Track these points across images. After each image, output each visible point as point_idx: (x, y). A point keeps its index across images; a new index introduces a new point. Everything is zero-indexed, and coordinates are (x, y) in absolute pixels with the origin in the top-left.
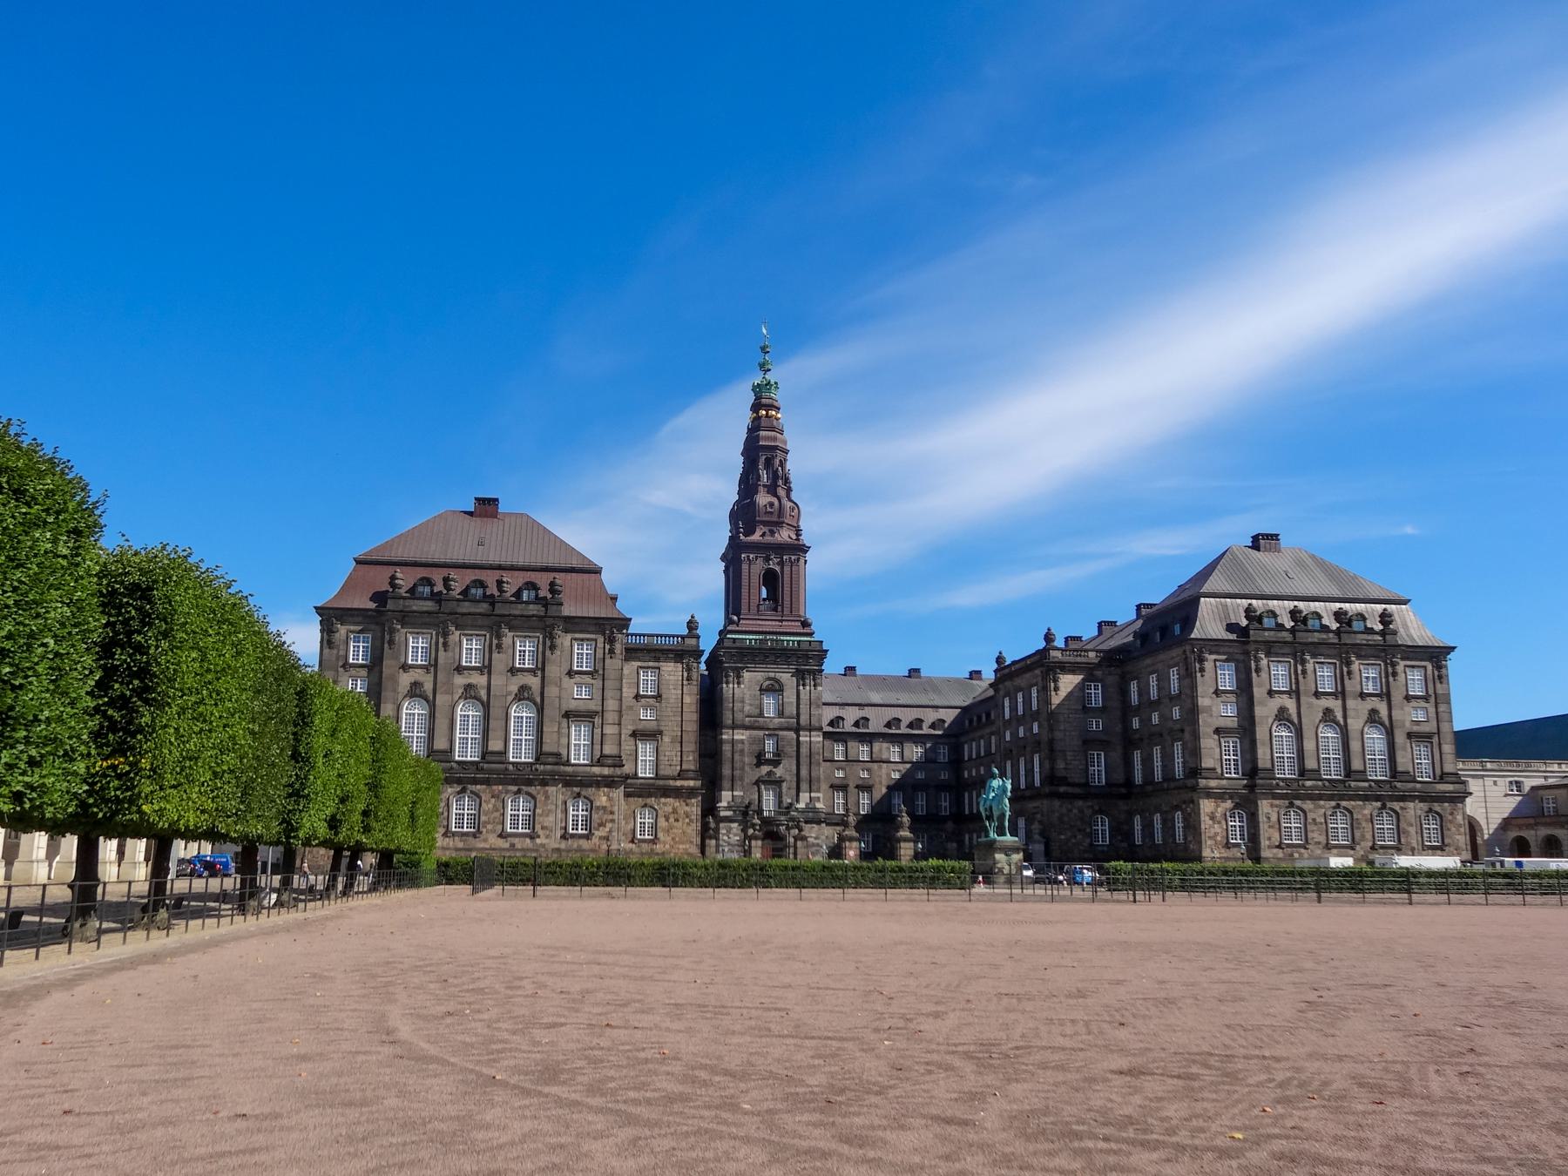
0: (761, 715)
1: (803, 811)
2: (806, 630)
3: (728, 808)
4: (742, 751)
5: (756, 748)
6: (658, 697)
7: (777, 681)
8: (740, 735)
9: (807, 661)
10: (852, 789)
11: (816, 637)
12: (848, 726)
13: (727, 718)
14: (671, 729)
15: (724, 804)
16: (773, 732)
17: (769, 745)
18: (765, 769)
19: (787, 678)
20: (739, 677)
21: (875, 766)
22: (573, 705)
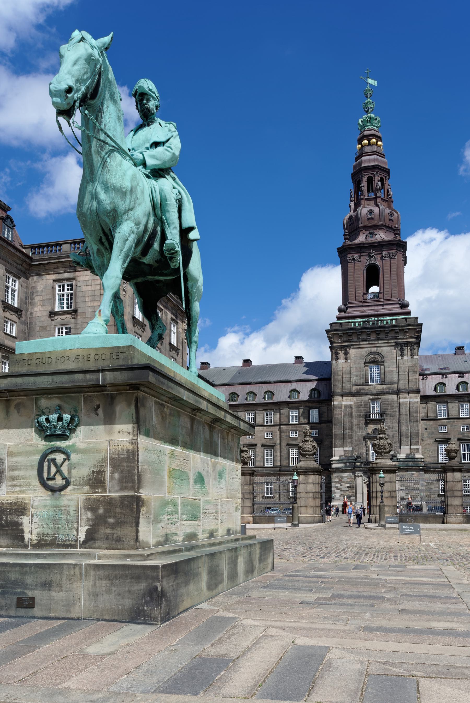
0: (366, 383)
1: (404, 461)
2: (404, 310)
3: (340, 461)
4: (351, 414)
5: (362, 410)
7: (379, 354)
8: (347, 401)
13: (338, 387)
17: (375, 408)
18: (371, 427)
19: (388, 351)
20: (346, 354)
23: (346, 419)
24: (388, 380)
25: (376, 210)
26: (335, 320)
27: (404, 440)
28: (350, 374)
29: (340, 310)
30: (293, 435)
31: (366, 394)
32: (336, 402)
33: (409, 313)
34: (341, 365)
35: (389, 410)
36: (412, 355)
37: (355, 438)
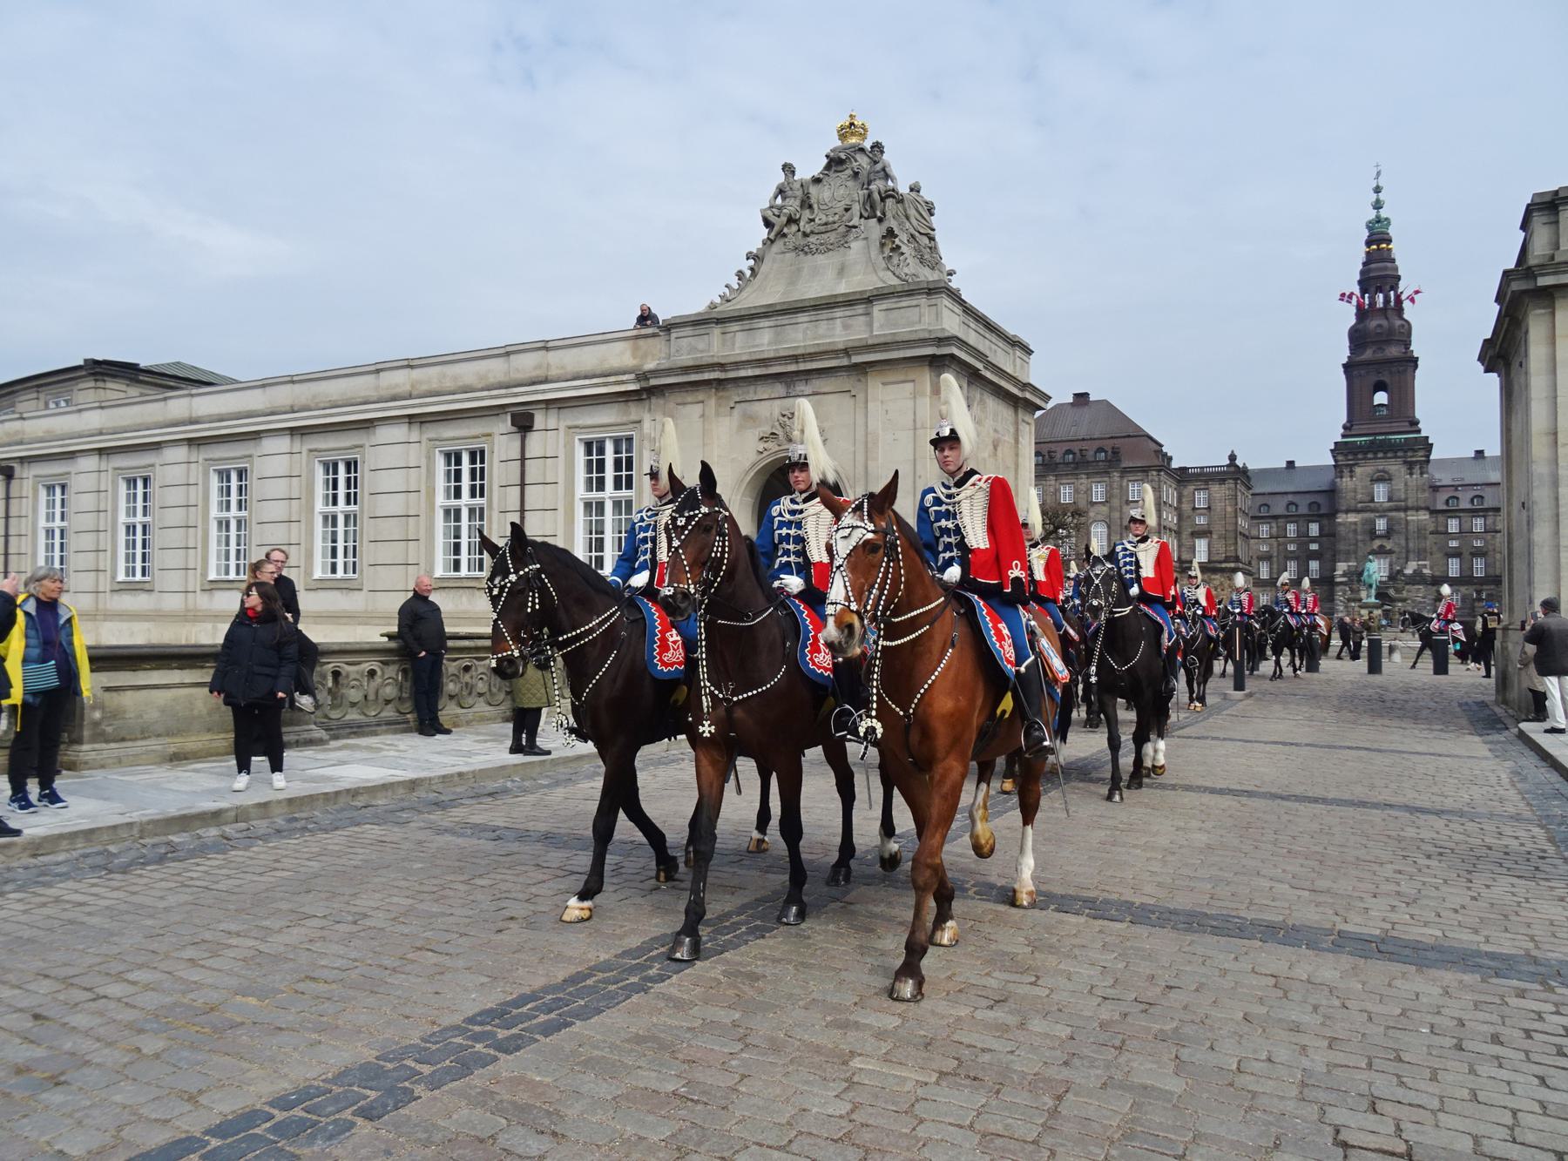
0: (1372, 500)
3: (1344, 575)
4: (1355, 531)
5: (1367, 527)
6: (1209, 508)
8: (1352, 518)
9: (1418, 450)
10: (1466, 555)
11: (1423, 434)
12: (1465, 505)
14: (1218, 529)
16: (1382, 512)
17: (1381, 525)
18: (1377, 543)
19: (1395, 467)
21: (1489, 536)
25: (1384, 323)
26: (1339, 439)
27: (1411, 556)
28: (1355, 491)
29: (1345, 427)
30: (1292, 547)
31: (1372, 511)
32: (1341, 518)
33: (1419, 431)
34: (1346, 483)
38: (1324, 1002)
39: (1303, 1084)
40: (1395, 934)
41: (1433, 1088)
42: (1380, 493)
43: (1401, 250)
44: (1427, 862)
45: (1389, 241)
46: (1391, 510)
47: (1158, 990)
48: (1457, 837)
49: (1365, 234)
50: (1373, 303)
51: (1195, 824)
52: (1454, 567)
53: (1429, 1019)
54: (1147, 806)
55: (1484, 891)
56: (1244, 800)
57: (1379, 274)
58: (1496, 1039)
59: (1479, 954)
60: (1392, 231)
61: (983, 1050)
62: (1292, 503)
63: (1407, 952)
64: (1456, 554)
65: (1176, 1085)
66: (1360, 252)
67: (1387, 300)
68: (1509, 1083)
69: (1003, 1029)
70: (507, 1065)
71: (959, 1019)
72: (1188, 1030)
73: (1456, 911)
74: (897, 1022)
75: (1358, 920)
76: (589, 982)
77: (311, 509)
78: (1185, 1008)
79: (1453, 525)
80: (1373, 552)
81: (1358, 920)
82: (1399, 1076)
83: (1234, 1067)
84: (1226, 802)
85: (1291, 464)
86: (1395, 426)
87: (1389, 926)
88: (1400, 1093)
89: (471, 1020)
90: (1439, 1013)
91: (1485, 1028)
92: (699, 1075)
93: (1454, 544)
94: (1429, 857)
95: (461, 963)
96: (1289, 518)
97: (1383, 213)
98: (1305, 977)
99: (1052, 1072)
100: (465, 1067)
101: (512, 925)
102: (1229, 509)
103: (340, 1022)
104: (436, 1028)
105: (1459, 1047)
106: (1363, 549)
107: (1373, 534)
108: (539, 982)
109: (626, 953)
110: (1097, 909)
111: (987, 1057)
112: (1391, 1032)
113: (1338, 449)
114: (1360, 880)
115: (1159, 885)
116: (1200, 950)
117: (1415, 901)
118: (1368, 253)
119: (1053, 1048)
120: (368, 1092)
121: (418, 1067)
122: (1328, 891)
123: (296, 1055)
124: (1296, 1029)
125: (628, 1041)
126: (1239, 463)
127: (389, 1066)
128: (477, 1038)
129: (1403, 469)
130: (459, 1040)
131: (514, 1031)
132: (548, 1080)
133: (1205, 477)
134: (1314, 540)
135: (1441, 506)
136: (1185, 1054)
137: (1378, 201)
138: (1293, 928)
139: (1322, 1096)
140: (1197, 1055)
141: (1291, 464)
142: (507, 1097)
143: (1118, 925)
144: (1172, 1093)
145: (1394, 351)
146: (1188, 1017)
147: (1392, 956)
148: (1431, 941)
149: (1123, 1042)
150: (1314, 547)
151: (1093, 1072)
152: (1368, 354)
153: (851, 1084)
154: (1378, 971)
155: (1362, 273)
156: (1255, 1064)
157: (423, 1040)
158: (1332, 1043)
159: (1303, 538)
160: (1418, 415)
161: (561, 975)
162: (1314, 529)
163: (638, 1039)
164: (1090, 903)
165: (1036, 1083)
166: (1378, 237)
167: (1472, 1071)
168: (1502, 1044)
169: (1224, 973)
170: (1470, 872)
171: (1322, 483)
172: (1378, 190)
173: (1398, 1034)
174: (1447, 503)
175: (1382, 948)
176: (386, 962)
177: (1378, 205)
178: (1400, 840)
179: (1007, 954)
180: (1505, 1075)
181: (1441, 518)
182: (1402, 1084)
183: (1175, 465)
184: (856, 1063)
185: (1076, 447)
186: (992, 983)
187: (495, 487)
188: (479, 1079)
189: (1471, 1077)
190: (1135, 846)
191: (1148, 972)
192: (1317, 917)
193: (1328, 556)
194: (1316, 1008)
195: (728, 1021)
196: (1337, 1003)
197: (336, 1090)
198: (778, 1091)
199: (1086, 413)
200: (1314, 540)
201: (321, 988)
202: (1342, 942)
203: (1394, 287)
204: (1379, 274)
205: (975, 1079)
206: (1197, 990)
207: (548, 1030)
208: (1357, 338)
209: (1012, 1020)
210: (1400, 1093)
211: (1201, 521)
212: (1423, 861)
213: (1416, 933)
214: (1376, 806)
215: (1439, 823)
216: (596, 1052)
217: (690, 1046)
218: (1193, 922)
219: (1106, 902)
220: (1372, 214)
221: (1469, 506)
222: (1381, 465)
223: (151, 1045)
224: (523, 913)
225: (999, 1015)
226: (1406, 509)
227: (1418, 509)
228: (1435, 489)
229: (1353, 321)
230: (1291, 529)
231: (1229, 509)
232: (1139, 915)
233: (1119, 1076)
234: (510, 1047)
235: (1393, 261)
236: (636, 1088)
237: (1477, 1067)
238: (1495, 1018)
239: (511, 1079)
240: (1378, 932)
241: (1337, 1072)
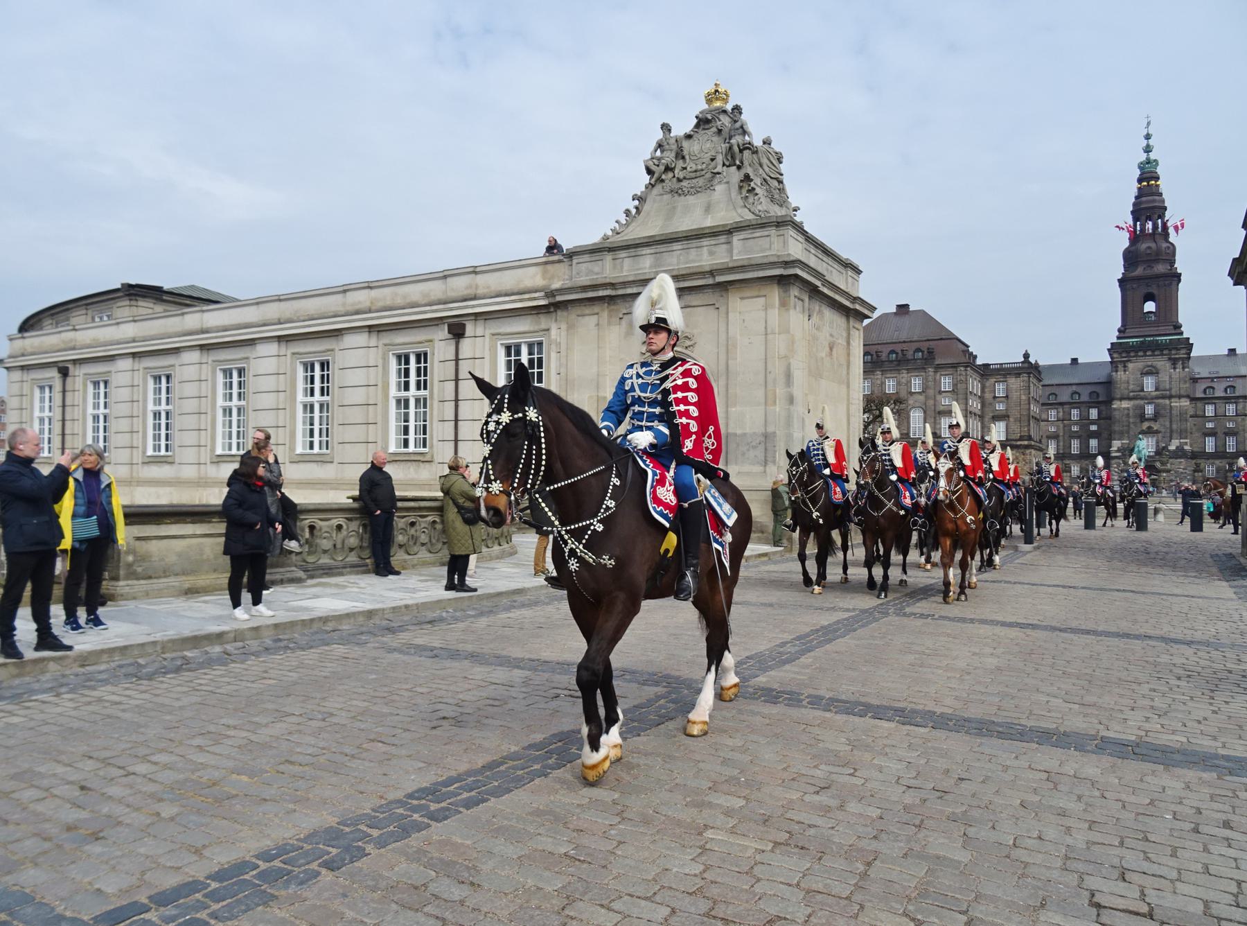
8: (1125, 404)
10: (1220, 435)
11: (1185, 336)
12: (1219, 393)
14: (1014, 413)
15: (1114, 448)
16: (1150, 400)
17: (1150, 410)
18: (1145, 425)
19: (1162, 363)
21: (1240, 419)
22: (942, 408)
23: (1124, 419)
24: (1161, 387)
25: (1153, 245)
26: (1115, 340)
27: (1175, 435)
29: (1119, 331)
30: (1075, 428)
31: (1142, 399)
33: (1182, 333)
34: (1120, 376)
35: (1162, 412)
36: (1183, 368)
37: (1132, 433)
38: (1087, 793)
39: (1067, 858)
40: (1148, 739)
41: (1172, 862)
42: (1149, 383)
43: (1166, 186)
44: (1178, 683)
45: (1157, 178)
46: (1157, 397)
47: (952, 782)
48: (1203, 663)
49: (1138, 172)
50: (1143, 230)
51: (988, 650)
52: (1210, 445)
53: (1173, 807)
54: (948, 635)
55: (1223, 706)
56: (1029, 631)
57: (1148, 205)
58: (1227, 825)
59: (1216, 756)
60: (1159, 170)
61: (810, 826)
62: (1076, 393)
63: (1158, 754)
64: (1212, 433)
65: (963, 856)
66: (1132, 189)
67: (1155, 227)
68: (1236, 860)
69: (827, 810)
70: (437, 830)
71: (791, 801)
72: (976, 813)
73: (1199, 722)
74: (742, 802)
75: (1118, 728)
76: (502, 768)
77: (85, 410)
78: (973, 795)
79: (1210, 410)
80: (1143, 432)
81: (1118, 728)
82: (1145, 852)
83: (1011, 842)
84: (1014, 633)
85: (1075, 361)
86: (1162, 330)
87: (1143, 733)
88: (1146, 866)
89: (410, 796)
90: (1180, 803)
91: (1219, 815)
92: (585, 840)
93: (1210, 425)
94: (1179, 678)
95: (404, 752)
96: (1073, 405)
97: (1152, 156)
98: (1072, 773)
99: (863, 844)
100: (406, 831)
101: (444, 723)
102: (1023, 397)
103: (311, 796)
104: (383, 802)
105: (1196, 830)
106: (1134, 430)
107: (1142, 417)
108: (463, 767)
109: (530, 746)
110: (905, 716)
111: (812, 831)
112: (1140, 818)
113: (1113, 349)
114: (1121, 696)
115: (957, 698)
116: (988, 751)
117: (1165, 714)
118: (1139, 189)
119: (866, 826)
120: (331, 849)
121: (369, 831)
122: (1094, 705)
123: (277, 820)
124: (1063, 814)
125: (531, 814)
126: (1032, 360)
127: (347, 829)
128: (415, 809)
129: (1168, 365)
130: (401, 811)
131: (443, 805)
132: (469, 842)
133: (1003, 372)
134: (1093, 422)
135: (1200, 395)
136: (972, 832)
137: (1148, 146)
138: (1065, 734)
139: (1081, 867)
140: (981, 832)
141: (1075, 361)
142: (436, 855)
143: (922, 730)
144: (960, 862)
145: (1161, 268)
146: (975, 803)
147: (1143, 757)
148: (1178, 746)
149: (922, 821)
150: (1094, 428)
151: (896, 845)
152: (1139, 271)
153: (704, 850)
154: (1132, 769)
155: (1134, 205)
156: (1028, 841)
157: (373, 810)
158: (1092, 824)
159: (1085, 421)
160: (1180, 321)
161: (480, 763)
162: (1094, 413)
163: (538, 813)
164: (900, 712)
165: (850, 853)
166: (1148, 175)
167: (1206, 850)
168: (1231, 828)
169: (1006, 768)
170: (1213, 691)
171: (1101, 376)
172: (1148, 137)
173: (1147, 819)
174: (1205, 391)
175: (1137, 750)
176: (347, 751)
177: (1148, 149)
178: (1156, 664)
179: (832, 751)
180: (1232, 853)
181: (1199, 404)
182: (1147, 859)
183: (979, 362)
184: (709, 834)
185: (898, 348)
186: (818, 773)
187: (336, 389)
188: (415, 840)
189: (1205, 854)
190: (938, 667)
191: (945, 767)
192: (1084, 725)
193: (1105, 435)
194: (1080, 798)
195: (609, 800)
196: (1097, 793)
197: (307, 847)
198: (646, 854)
199: (906, 321)
200: (1093, 422)
201: (297, 769)
202: (1104, 745)
203: (1161, 216)
204: (1148, 205)
205: (802, 848)
206: (983, 782)
207: (469, 804)
208: (1131, 258)
209: (834, 803)
210: (1146, 866)
211: (1000, 407)
212: (1174, 682)
213: (1165, 739)
214: (1137, 637)
215: (1189, 651)
216: (506, 822)
217: (579, 818)
218: (983, 728)
219: (914, 711)
220: (1143, 157)
221: (1223, 394)
222: (1150, 361)
223: (167, 810)
224: (452, 714)
225: (823, 798)
226: (1170, 397)
227: (1180, 397)
228: (1195, 380)
229: (1127, 244)
230: (1075, 412)
231: (1023, 397)
232: (940, 722)
233: (917, 848)
234: (436, 817)
235: (1161, 194)
236: (536, 850)
237: (1210, 847)
238: (1227, 808)
239: (439, 842)
240: (1133, 738)
241: (1095, 848)
